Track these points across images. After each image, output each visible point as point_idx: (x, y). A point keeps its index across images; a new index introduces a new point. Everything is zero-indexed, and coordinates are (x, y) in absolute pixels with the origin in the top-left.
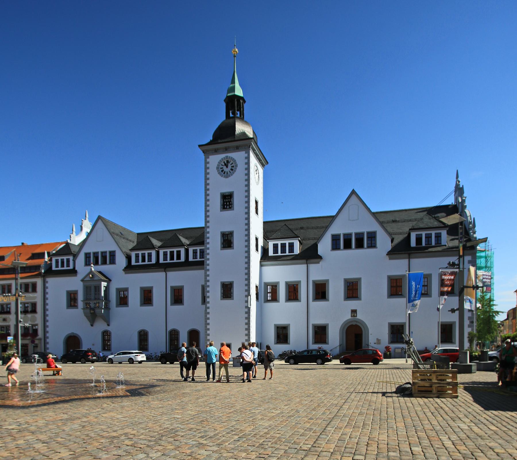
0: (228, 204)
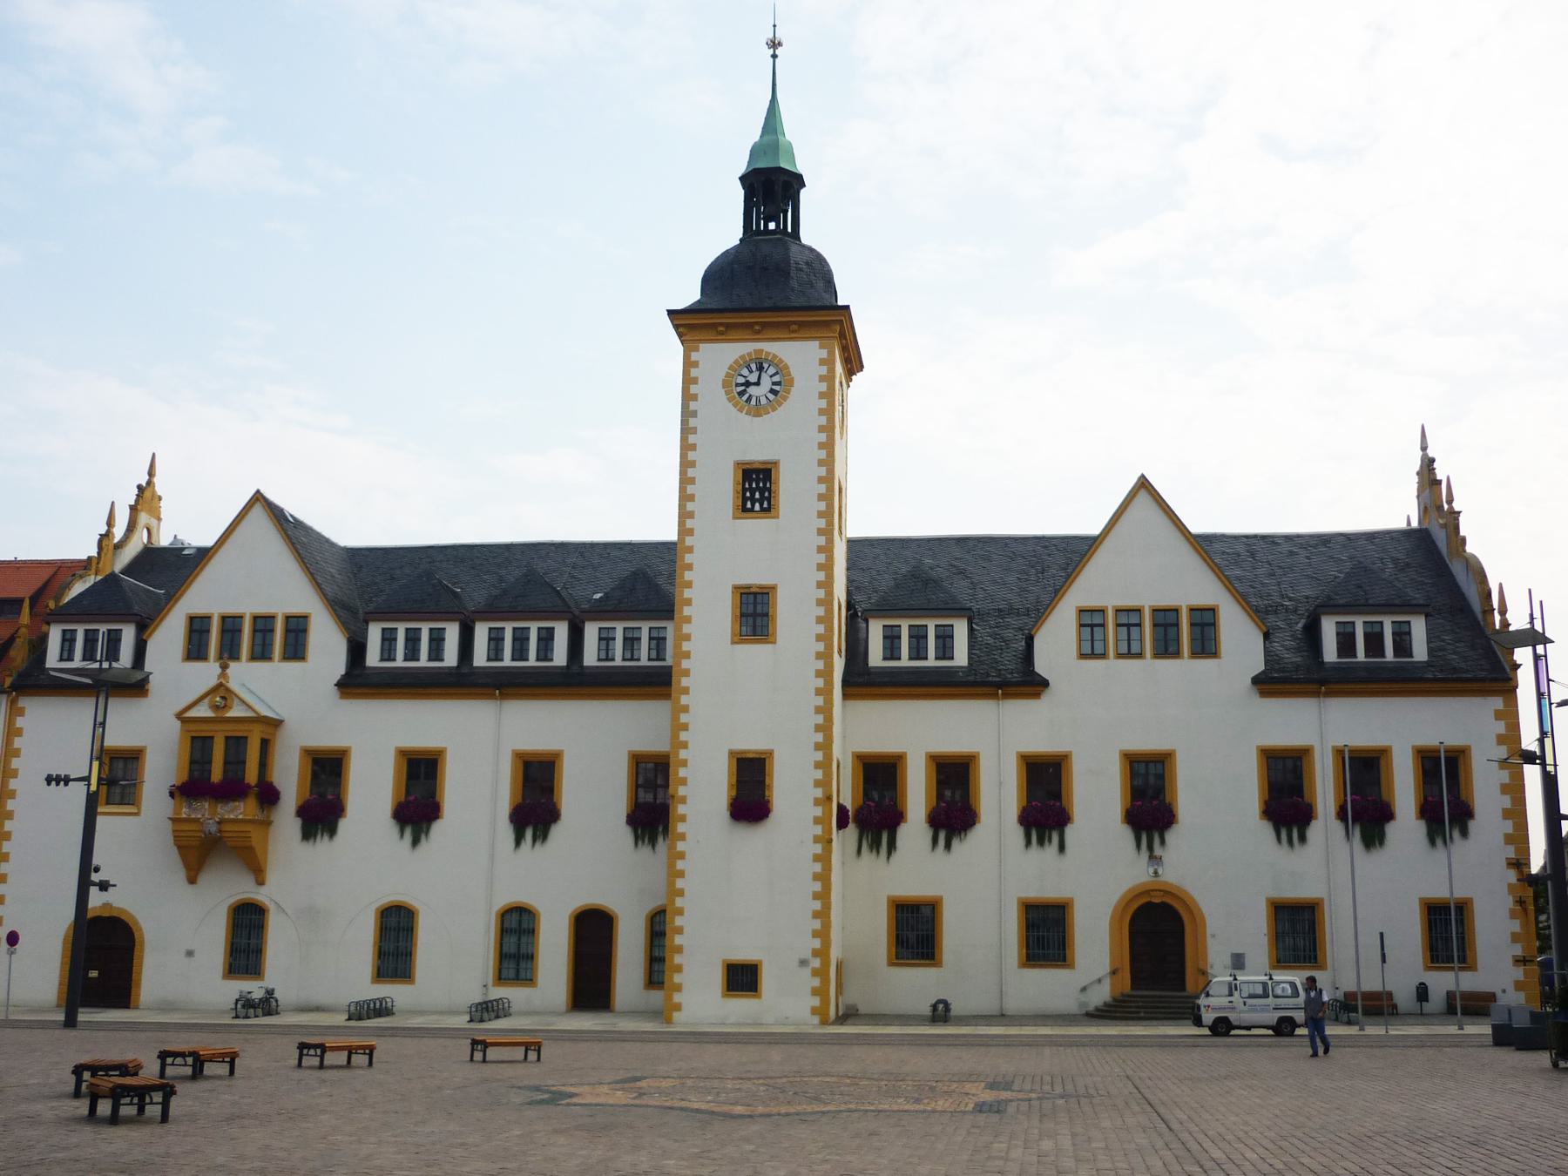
0: (757, 496)
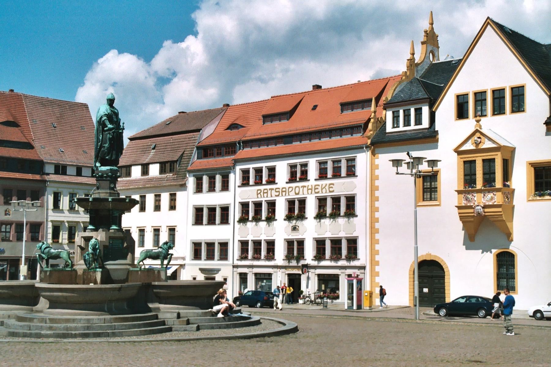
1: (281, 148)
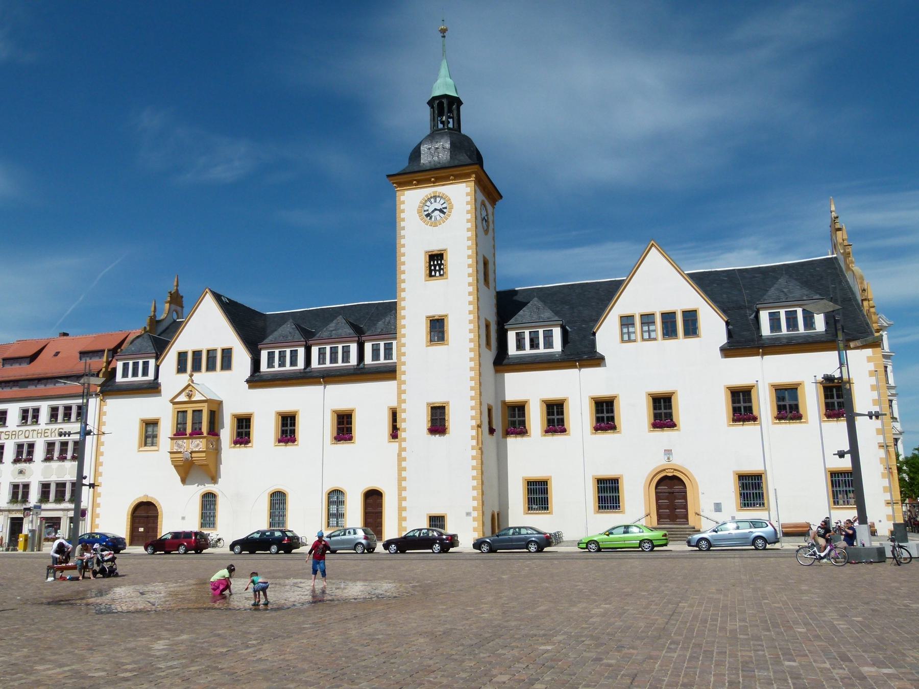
0: (437, 268)
1: (15, 391)
